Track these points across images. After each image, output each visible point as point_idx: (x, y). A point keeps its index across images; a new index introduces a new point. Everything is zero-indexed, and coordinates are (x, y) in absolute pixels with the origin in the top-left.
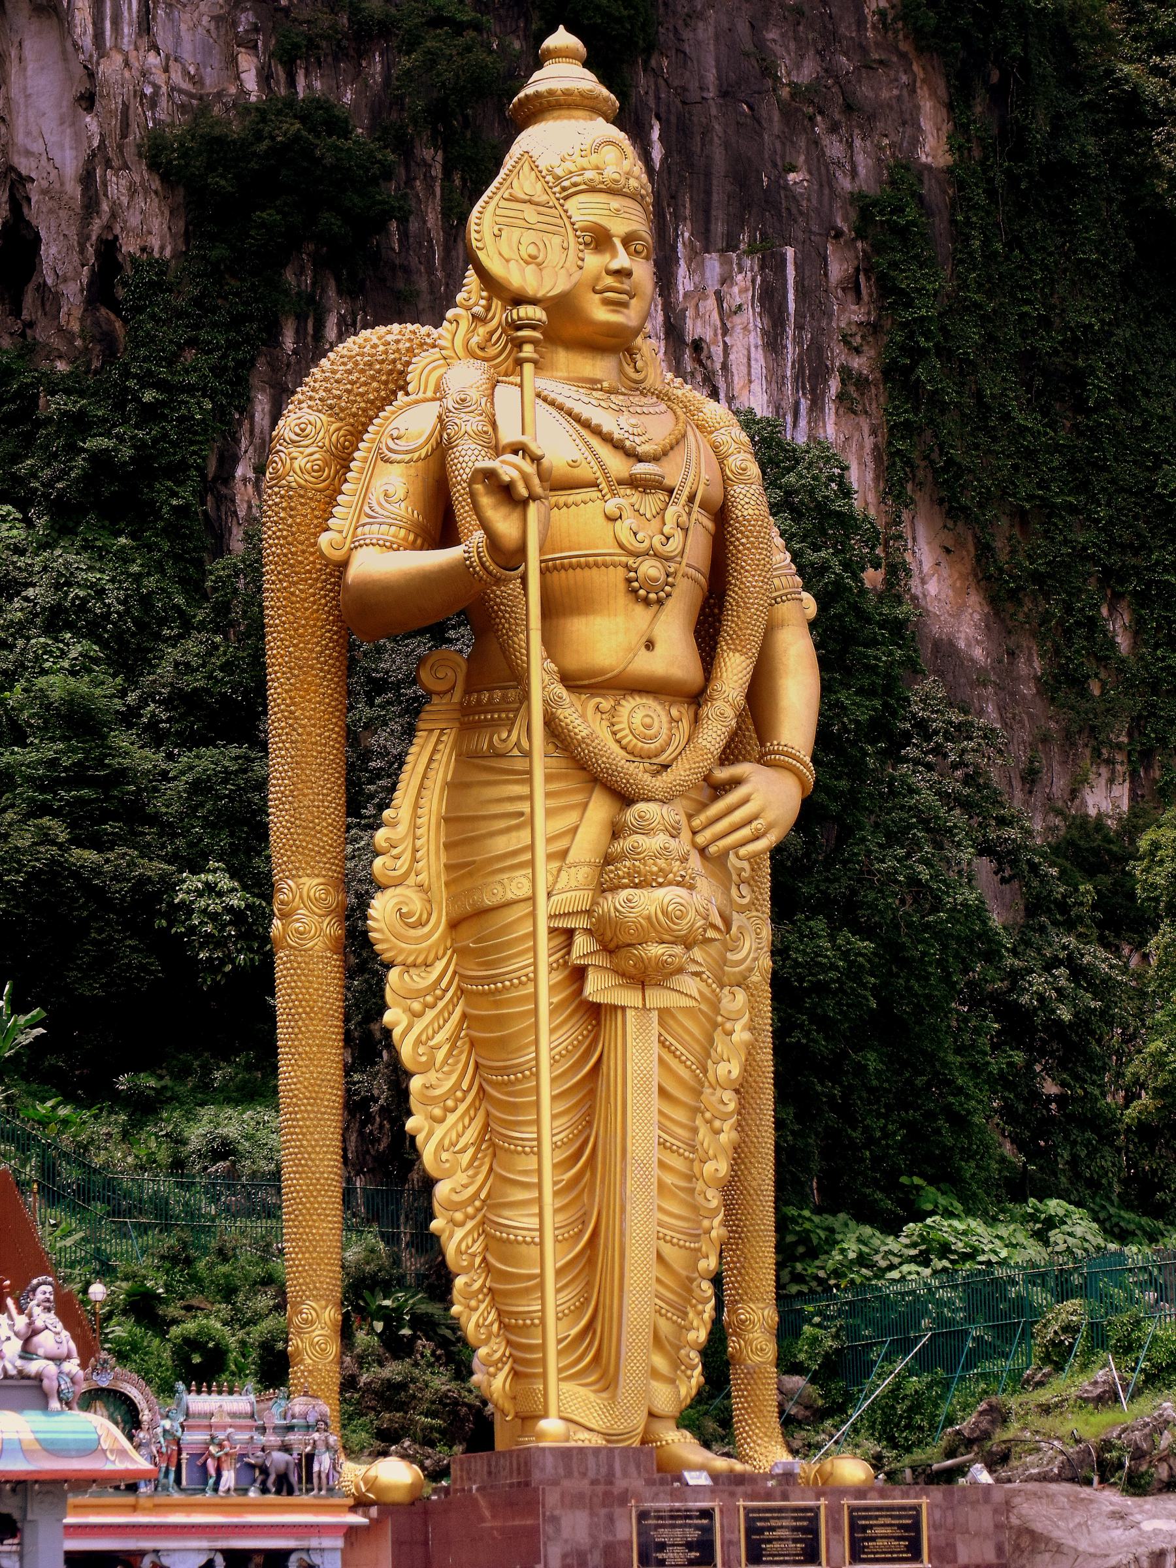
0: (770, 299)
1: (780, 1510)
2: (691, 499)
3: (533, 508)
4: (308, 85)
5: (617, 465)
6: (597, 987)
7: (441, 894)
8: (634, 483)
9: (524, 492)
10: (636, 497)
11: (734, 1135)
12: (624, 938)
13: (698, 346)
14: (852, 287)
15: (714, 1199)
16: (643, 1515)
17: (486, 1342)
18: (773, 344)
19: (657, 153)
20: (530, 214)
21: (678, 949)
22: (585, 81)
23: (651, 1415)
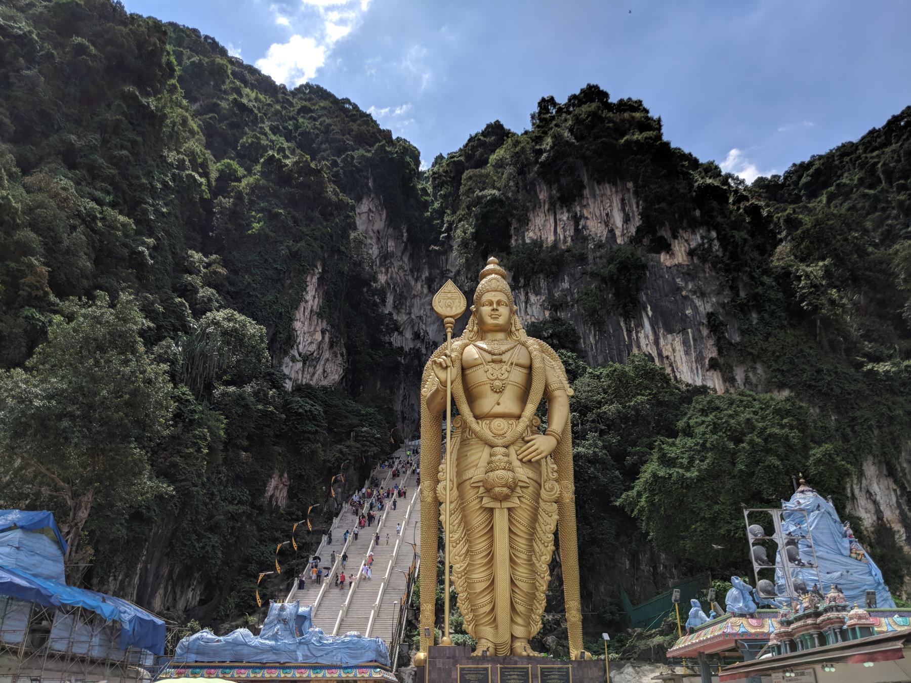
0: (685, 343)
1: (514, 668)
2: (512, 364)
3: (449, 369)
4: (562, 315)
5: (489, 357)
6: (487, 502)
7: (455, 480)
8: (493, 361)
9: (444, 365)
10: (493, 365)
11: (553, 548)
12: (489, 487)
13: (667, 357)
14: (709, 337)
15: (545, 567)
16: (462, 669)
17: (467, 614)
18: (687, 353)
19: (650, 313)
20: (449, 295)
21: (505, 489)
22: (498, 268)
23: (512, 635)
